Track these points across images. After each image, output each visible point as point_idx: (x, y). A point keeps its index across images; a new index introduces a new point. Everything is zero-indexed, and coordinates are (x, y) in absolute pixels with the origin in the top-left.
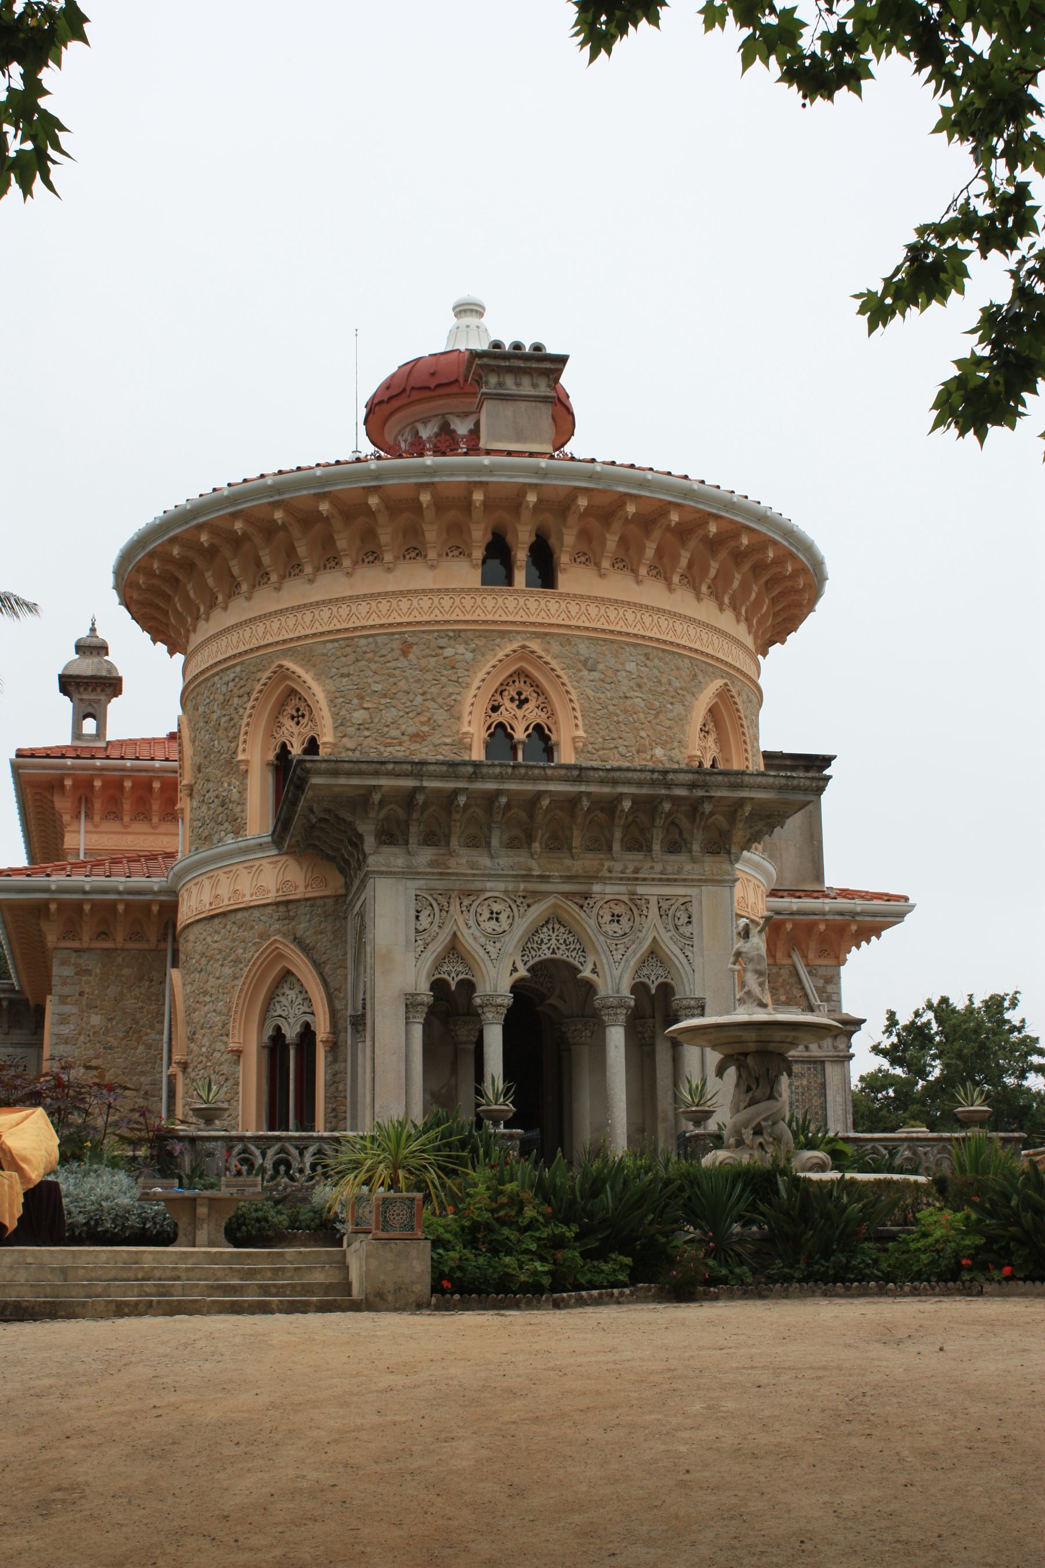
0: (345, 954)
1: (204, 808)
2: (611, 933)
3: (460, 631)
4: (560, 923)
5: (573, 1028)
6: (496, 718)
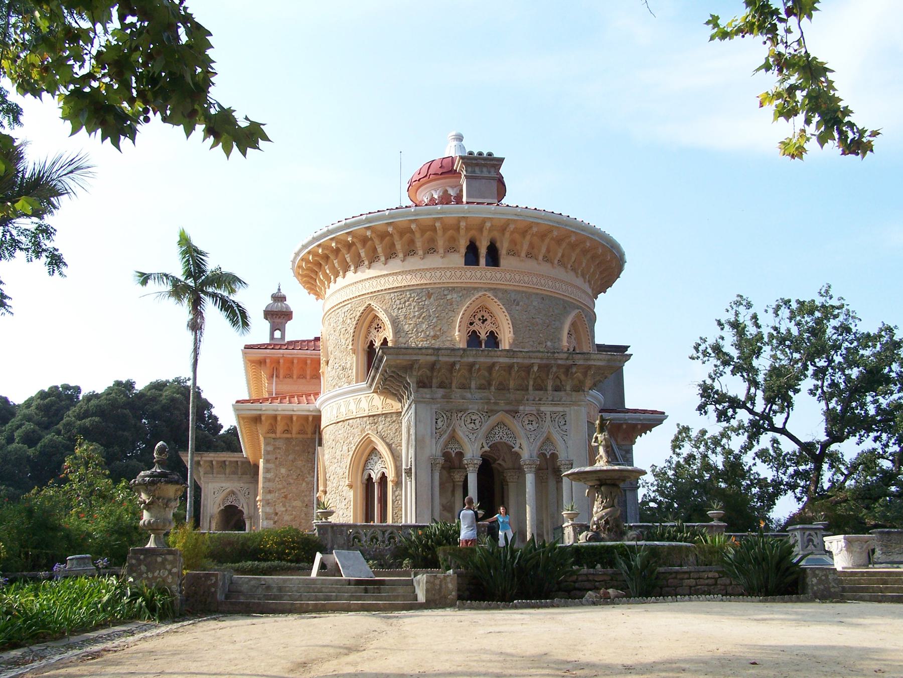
0: (401, 440)
1: (334, 371)
2: (528, 429)
3: (455, 287)
4: (504, 425)
5: (509, 474)
6: (472, 328)
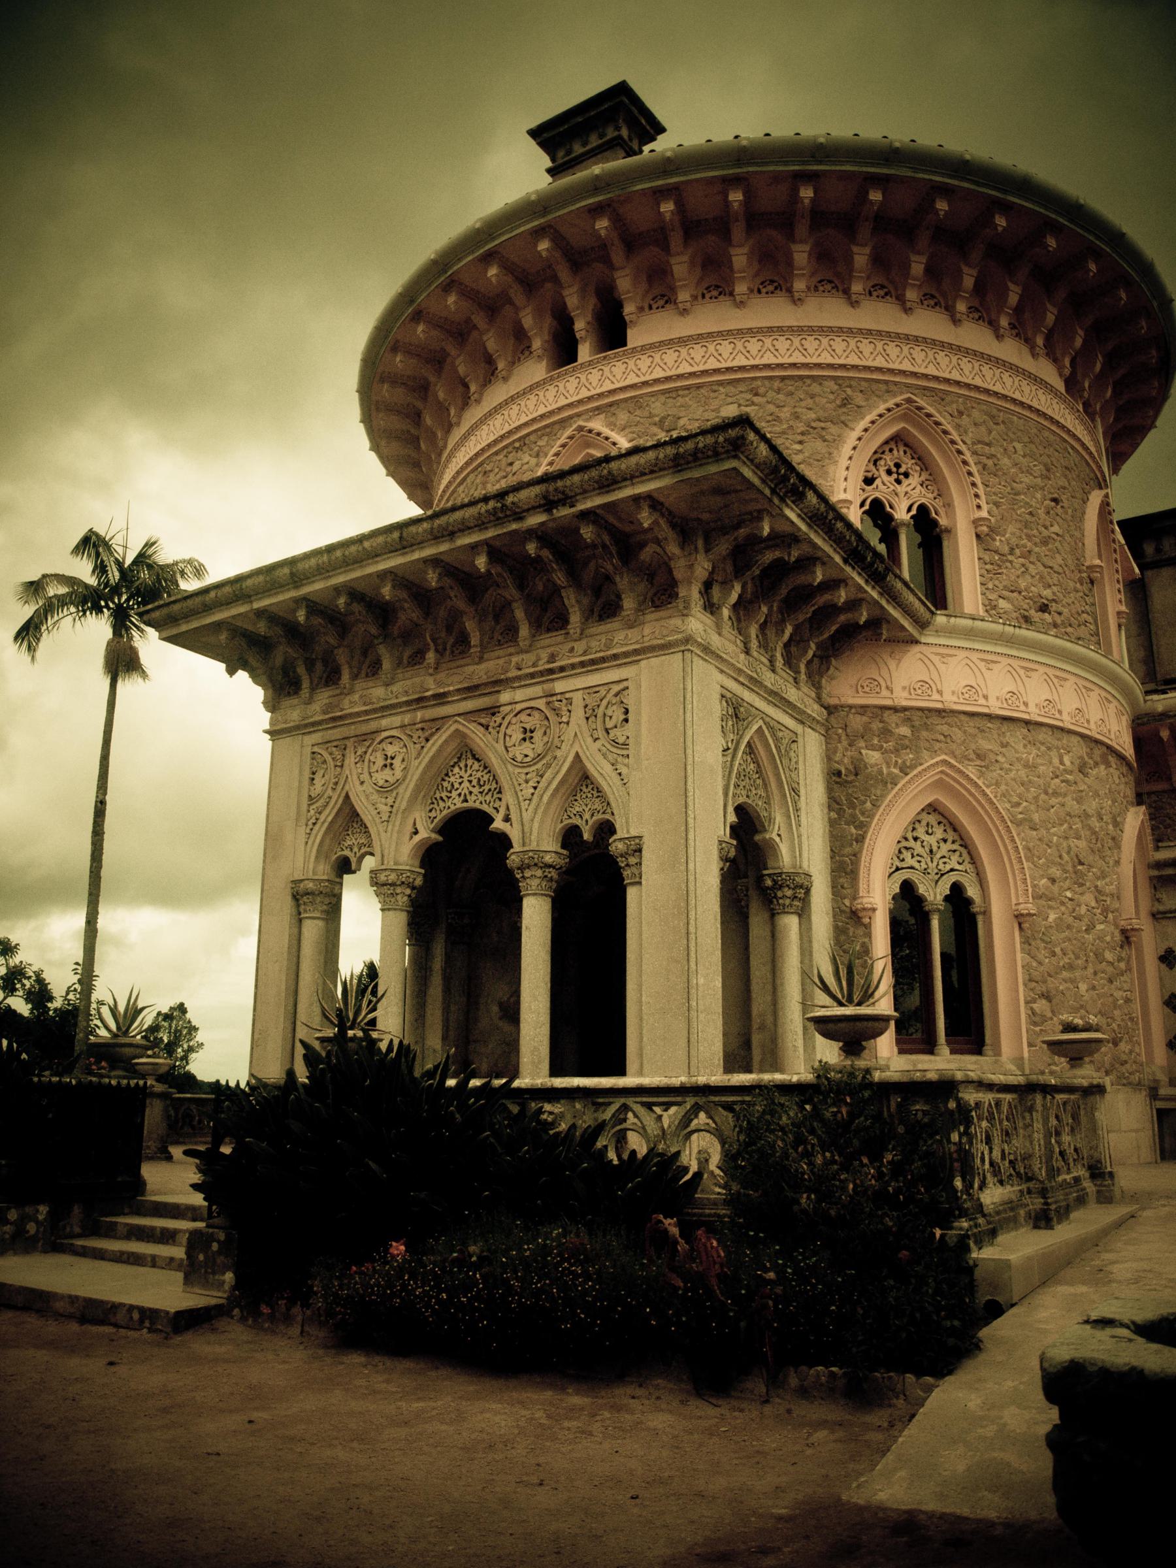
4: (474, 756)
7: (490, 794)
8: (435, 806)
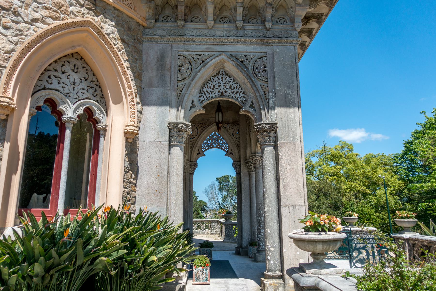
4: (227, 74)
7: (238, 94)
8: (203, 94)
